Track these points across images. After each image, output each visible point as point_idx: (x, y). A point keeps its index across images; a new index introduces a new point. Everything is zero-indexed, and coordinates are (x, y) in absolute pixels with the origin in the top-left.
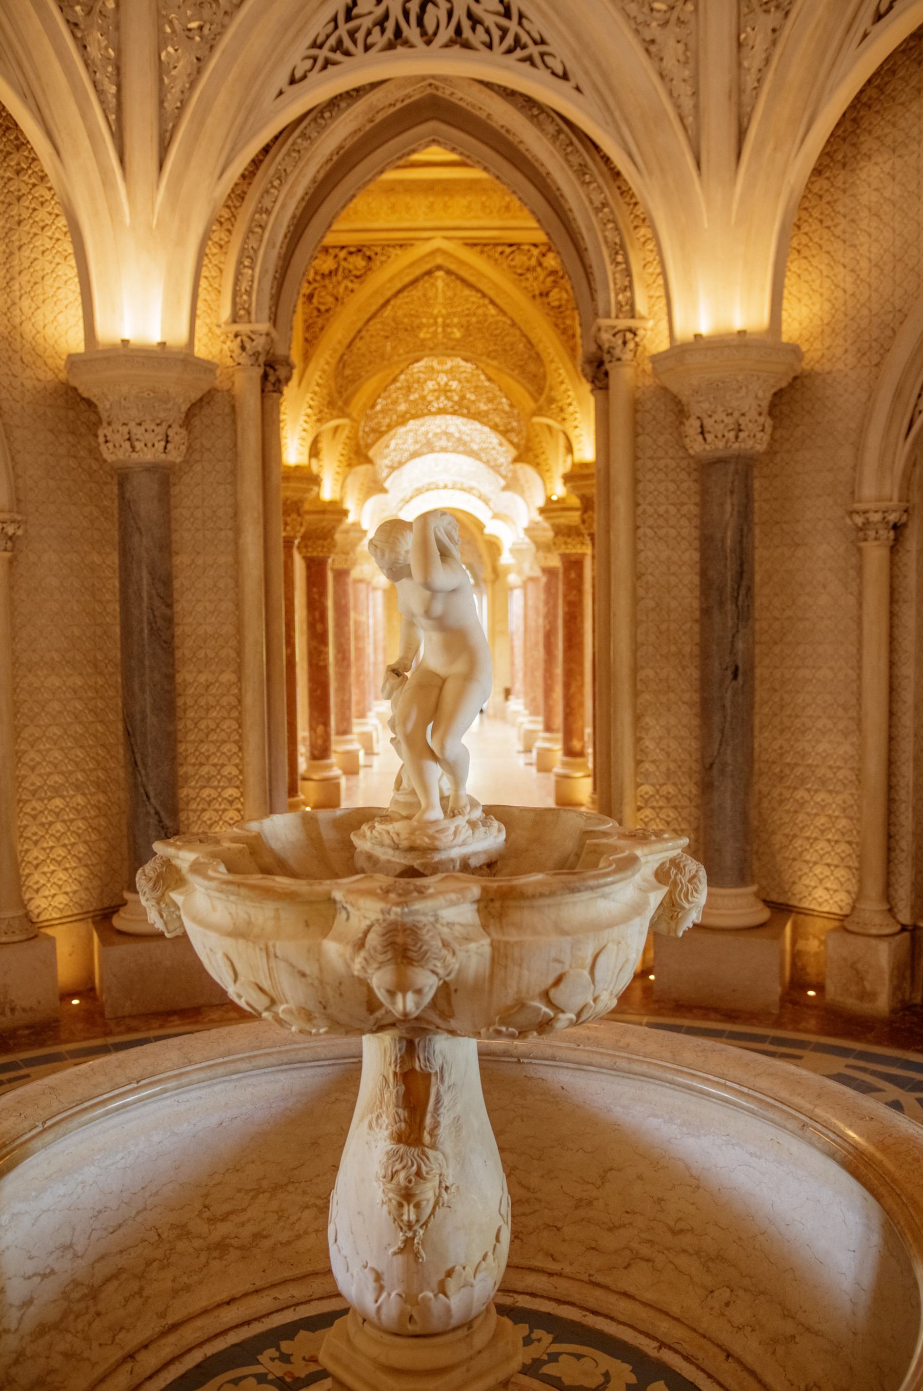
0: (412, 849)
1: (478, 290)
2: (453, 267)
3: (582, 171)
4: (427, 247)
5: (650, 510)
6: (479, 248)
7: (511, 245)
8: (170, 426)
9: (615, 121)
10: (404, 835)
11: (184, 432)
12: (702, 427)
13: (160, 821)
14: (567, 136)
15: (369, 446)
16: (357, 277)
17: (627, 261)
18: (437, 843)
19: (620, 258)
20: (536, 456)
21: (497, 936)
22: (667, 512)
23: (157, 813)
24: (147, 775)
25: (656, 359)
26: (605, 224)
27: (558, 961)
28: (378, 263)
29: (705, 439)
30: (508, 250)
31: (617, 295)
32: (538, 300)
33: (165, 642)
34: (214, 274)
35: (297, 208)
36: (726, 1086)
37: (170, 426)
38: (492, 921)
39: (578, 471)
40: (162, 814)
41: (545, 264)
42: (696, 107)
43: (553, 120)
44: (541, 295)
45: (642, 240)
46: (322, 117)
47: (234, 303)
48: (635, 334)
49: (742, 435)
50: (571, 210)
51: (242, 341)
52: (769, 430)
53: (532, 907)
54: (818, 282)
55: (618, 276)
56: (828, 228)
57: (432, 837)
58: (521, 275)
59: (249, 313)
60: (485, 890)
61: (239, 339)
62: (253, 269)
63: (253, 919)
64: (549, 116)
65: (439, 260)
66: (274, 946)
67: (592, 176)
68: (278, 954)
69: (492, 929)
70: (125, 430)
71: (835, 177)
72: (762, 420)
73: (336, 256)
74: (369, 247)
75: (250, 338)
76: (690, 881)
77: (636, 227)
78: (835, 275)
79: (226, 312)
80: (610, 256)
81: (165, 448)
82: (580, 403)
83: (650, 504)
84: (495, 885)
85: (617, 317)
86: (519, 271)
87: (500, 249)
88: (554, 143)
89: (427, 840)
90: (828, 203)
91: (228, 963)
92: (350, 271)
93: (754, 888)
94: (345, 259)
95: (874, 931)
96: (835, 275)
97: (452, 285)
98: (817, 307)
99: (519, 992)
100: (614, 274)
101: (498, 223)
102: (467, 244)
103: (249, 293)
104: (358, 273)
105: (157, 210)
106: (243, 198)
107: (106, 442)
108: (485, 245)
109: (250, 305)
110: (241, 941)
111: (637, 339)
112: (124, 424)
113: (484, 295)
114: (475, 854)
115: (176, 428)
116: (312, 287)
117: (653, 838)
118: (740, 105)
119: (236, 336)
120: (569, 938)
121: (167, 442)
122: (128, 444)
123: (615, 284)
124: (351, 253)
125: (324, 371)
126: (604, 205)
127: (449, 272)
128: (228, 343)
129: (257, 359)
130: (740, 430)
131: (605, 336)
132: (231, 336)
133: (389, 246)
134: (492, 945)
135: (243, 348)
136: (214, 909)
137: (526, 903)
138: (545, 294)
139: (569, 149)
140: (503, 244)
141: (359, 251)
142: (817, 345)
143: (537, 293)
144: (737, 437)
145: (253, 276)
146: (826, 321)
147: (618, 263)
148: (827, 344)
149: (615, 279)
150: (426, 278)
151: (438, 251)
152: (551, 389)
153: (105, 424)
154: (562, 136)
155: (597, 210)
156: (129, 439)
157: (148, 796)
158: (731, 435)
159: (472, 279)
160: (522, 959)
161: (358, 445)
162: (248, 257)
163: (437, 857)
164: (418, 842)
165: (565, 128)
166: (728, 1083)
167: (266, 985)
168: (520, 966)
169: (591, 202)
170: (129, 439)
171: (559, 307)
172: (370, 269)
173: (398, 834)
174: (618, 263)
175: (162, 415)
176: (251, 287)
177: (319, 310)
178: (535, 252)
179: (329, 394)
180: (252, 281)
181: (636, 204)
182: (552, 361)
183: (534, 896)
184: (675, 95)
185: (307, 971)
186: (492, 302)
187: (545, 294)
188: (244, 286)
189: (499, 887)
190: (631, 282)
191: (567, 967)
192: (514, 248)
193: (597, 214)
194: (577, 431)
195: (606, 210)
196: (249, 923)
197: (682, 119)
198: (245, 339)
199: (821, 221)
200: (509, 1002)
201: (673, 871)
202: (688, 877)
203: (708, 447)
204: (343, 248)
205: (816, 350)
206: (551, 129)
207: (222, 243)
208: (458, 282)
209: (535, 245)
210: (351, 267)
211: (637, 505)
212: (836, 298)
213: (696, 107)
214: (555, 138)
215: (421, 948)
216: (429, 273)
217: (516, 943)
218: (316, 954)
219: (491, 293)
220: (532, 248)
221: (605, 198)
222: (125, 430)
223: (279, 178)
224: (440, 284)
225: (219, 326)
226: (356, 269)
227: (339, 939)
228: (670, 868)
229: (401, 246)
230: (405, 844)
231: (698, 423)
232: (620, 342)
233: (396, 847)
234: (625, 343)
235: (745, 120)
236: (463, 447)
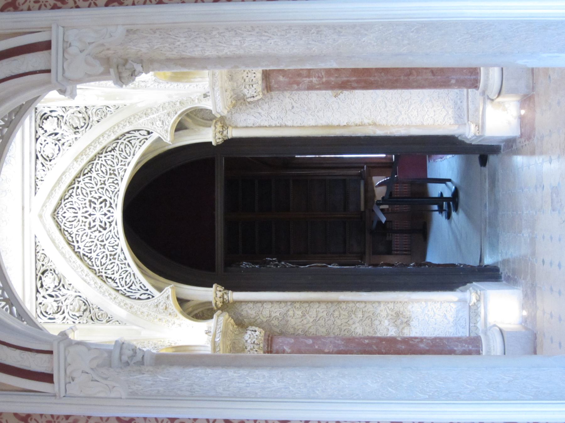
6: (39, 183)
58: (59, 150)
73: (44, 297)
104: (57, 279)
116: (67, 316)
124: (42, 286)
141: (40, 279)
172: (55, 271)
177: (85, 310)
204: (38, 291)
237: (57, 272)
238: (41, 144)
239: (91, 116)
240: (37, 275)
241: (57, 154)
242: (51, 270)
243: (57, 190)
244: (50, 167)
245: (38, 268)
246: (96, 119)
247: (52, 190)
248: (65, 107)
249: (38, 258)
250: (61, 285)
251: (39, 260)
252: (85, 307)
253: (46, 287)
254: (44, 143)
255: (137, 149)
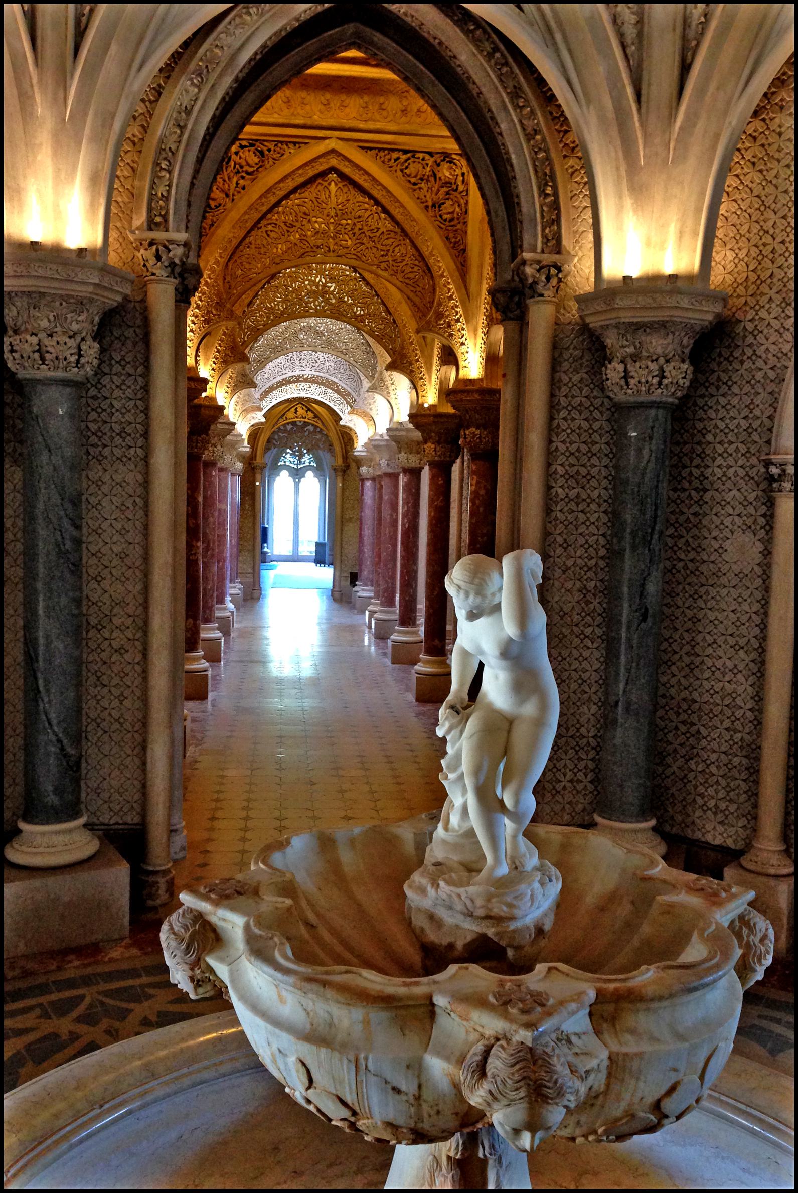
0: (488, 917)
1: (371, 197)
2: (347, 170)
3: (516, 94)
4: (322, 147)
5: (562, 447)
7: (405, 152)
8: (83, 339)
9: (555, 44)
10: (479, 902)
11: (97, 345)
12: (626, 371)
13: (62, 749)
14: (503, 55)
15: (245, 344)
16: (248, 173)
17: (556, 194)
18: (516, 912)
19: (549, 190)
20: (411, 364)
21: (615, 1047)
22: (578, 450)
23: (59, 741)
24: (50, 702)
25: (582, 300)
26: (536, 153)
27: (675, 1070)
28: (271, 160)
29: (627, 384)
30: (404, 157)
31: (543, 230)
32: (431, 213)
33: (73, 564)
34: (126, 173)
35: (217, 109)
36: (722, 1101)
37: (83, 339)
38: (605, 1025)
39: (461, 387)
40: (65, 742)
41: (439, 175)
42: (640, 34)
43: (489, 36)
44: (434, 205)
45: (570, 170)
46: (250, 14)
47: (150, 209)
48: (559, 270)
49: (665, 381)
50: (501, 134)
51: (157, 250)
52: (690, 376)
53: (648, 1010)
54: (746, 227)
55: (545, 208)
56: (761, 171)
57: (510, 906)
58: (415, 184)
59: (165, 217)
60: (599, 993)
61: (155, 247)
62: (170, 172)
63: (336, 1021)
64: (485, 31)
65: (334, 162)
66: (366, 1059)
67: (526, 100)
68: (371, 1066)
69: (606, 1036)
70: (34, 340)
71: (771, 120)
72: (685, 366)
74: (262, 142)
75: (165, 247)
76: (762, 940)
77: (565, 156)
78: (765, 221)
79: (140, 219)
80: (539, 187)
81: (78, 361)
82: (467, 321)
83: (563, 442)
84: (612, 986)
85: (543, 252)
86: (413, 180)
87: (395, 155)
88: (488, 61)
89: (505, 908)
90: (763, 145)
91: (303, 1070)
92: (242, 167)
93: (653, 822)
94: (237, 153)
95: (772, 871)
96: (765, 221)
97: (345, 190)
98: (744, 252)
99: (630, 1105)
100: (541, 206)
101: (393, 128)
102: (362, 148)
103: (166, 198)
104: (251, 169)
105: (70, 102)
106: (160, 94)
107: (12, 351)
108: (380, 149)
109: (167, 212)
110: (323, 1051)
111: (560, 276)
112: (32, 334)
113: (377, 203)
114: (545, 915)
115: (89, 341)
117: (724, 895)
118: (684, 38)
119: (151, 244)
120: (686, 1045)
121: (80, 356)
122: (37, 355)
123: (543, 217)
124: (242, 147)
125: (213, 272)
126: (536, 132)
127: (342, 176)
128: (142, 251)
129: (172, 272)
130: (665, 377)
131: (528, 270)
132: (146, 244)
133: (281, 142)
134: (610, 1058)
135: (158, 258)
136: (282, 1000)
137: (641, 1006)
138: (438, 205)
139: (505, 70)
140: (399, 150)
141: (251, 145)
142: (741, 290)
143: (430, 204)
144: (660, 383)
145: (170, 180)
146: (751, 268)
147: (547, 195)
148: (750, 292)
149: (542, 211)
150: (320, 181)
151: (333, 151)
152: (440, 304)
153: (10, 332)
154: (498, 55)
155: (529, 137)
156: (38, 351)
157: (50, 724)
158: (655, 381)
159: (366, 185)
160: (640, 1071)
161: (234, 341)
162: (165, 159)
163: (513, 926)
164: (495, 910)
165: (502, 47)
166: (723, 1098)
167: (349, 1099)
168: (638, 1079)
169: (524, 129)
170: (38, 351)
171: (452, 220)
172: (261, 166)
173: (472, 901)
174: (547, 195)
175: (75, 327)
176: (169, 191)
178: (430, 161)
179: (218, 294)
180: (170, 186)
181: (566, 132)
182: (442, 276)
183: (652, 1000)
184: (619, 21)
185: (404, 1088)
186: (385, 211)
187: (438, 205)
188: (161, 190)
189: (616, 989)
190: (559, 216)
191: (681, 1076)
192: (409, 155)
193: (528, 141)
194: (464, 348)
195: (538, 137)
196: (331, 1025)
197: (624, 47)
198: (160, 248)
199: (754, 163)
200: (618, 1113)
201: (745, 931)
202: (760, 935)
203: (630, 392)
205: (739, 296)
206: (488, 47)
207: (136, 140)
208: (351, 187)
209: (431, 154)
210: (244, 163)
211: (550, 442)
212: (765, 245)
213: (640, 34)
214: (490, 56)
215: (556, 1082)
216: (323, 174)
217: (636, 1054)
218: (416, 1067)
219: (383, 201)
220: (427, 157)
221: (538, 124)
222: (34, 340)
223: (200, 75)
224: (333, 187)
225: (133, 232)
226: (248, 164)
227: (441, 1053)
228: (741, 928)
229: (295, 144)
230: (480, 912)
231: (621, 367)
232: (543, 278)
233: (470, 914)
234: (548, 279)
235: (689, 54)
236: (329, 345)
237: (260, 169)
238: (423, 159)
239: (455, 228)
240: (257, 141)
241: (409, 181)
242: (263, 161)
243: (363, 177)
244: (393, 169)
245: (266, 144)
246: (451, 235)
247: (364, 170)
248: (467, 194)
249: (280, 145)
250: (244, 174)
251: (276, 145)
252: (213, 206)
253: (241, 153)
254: (424, 162)
255: (412, 289)
